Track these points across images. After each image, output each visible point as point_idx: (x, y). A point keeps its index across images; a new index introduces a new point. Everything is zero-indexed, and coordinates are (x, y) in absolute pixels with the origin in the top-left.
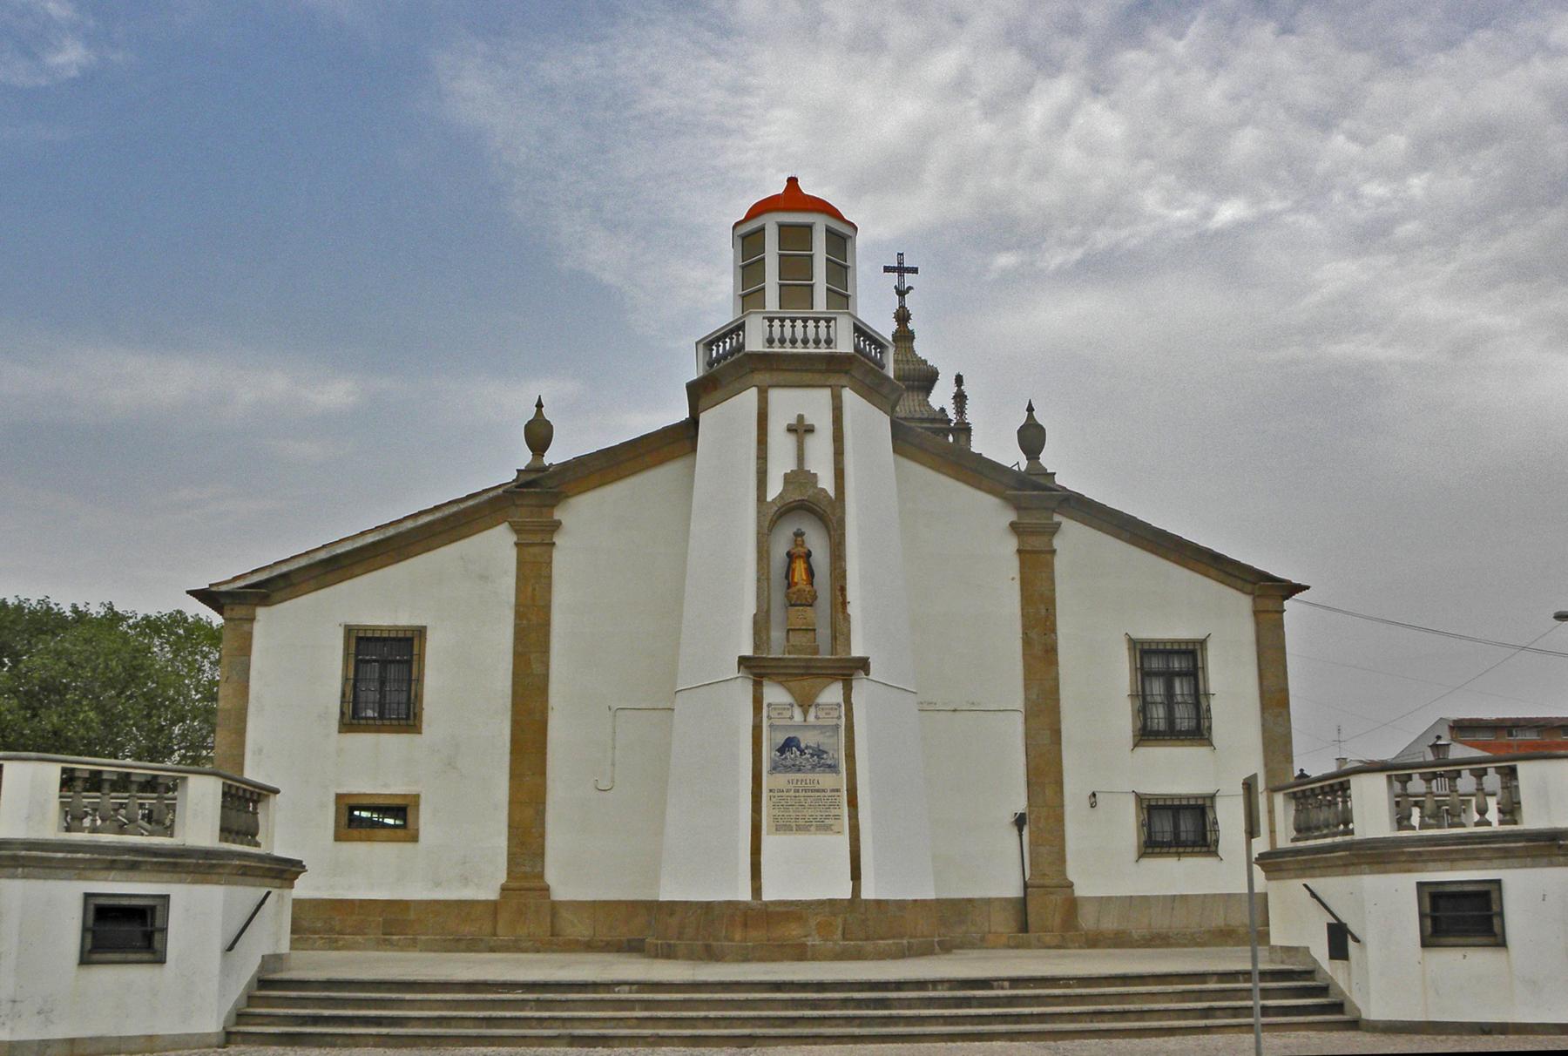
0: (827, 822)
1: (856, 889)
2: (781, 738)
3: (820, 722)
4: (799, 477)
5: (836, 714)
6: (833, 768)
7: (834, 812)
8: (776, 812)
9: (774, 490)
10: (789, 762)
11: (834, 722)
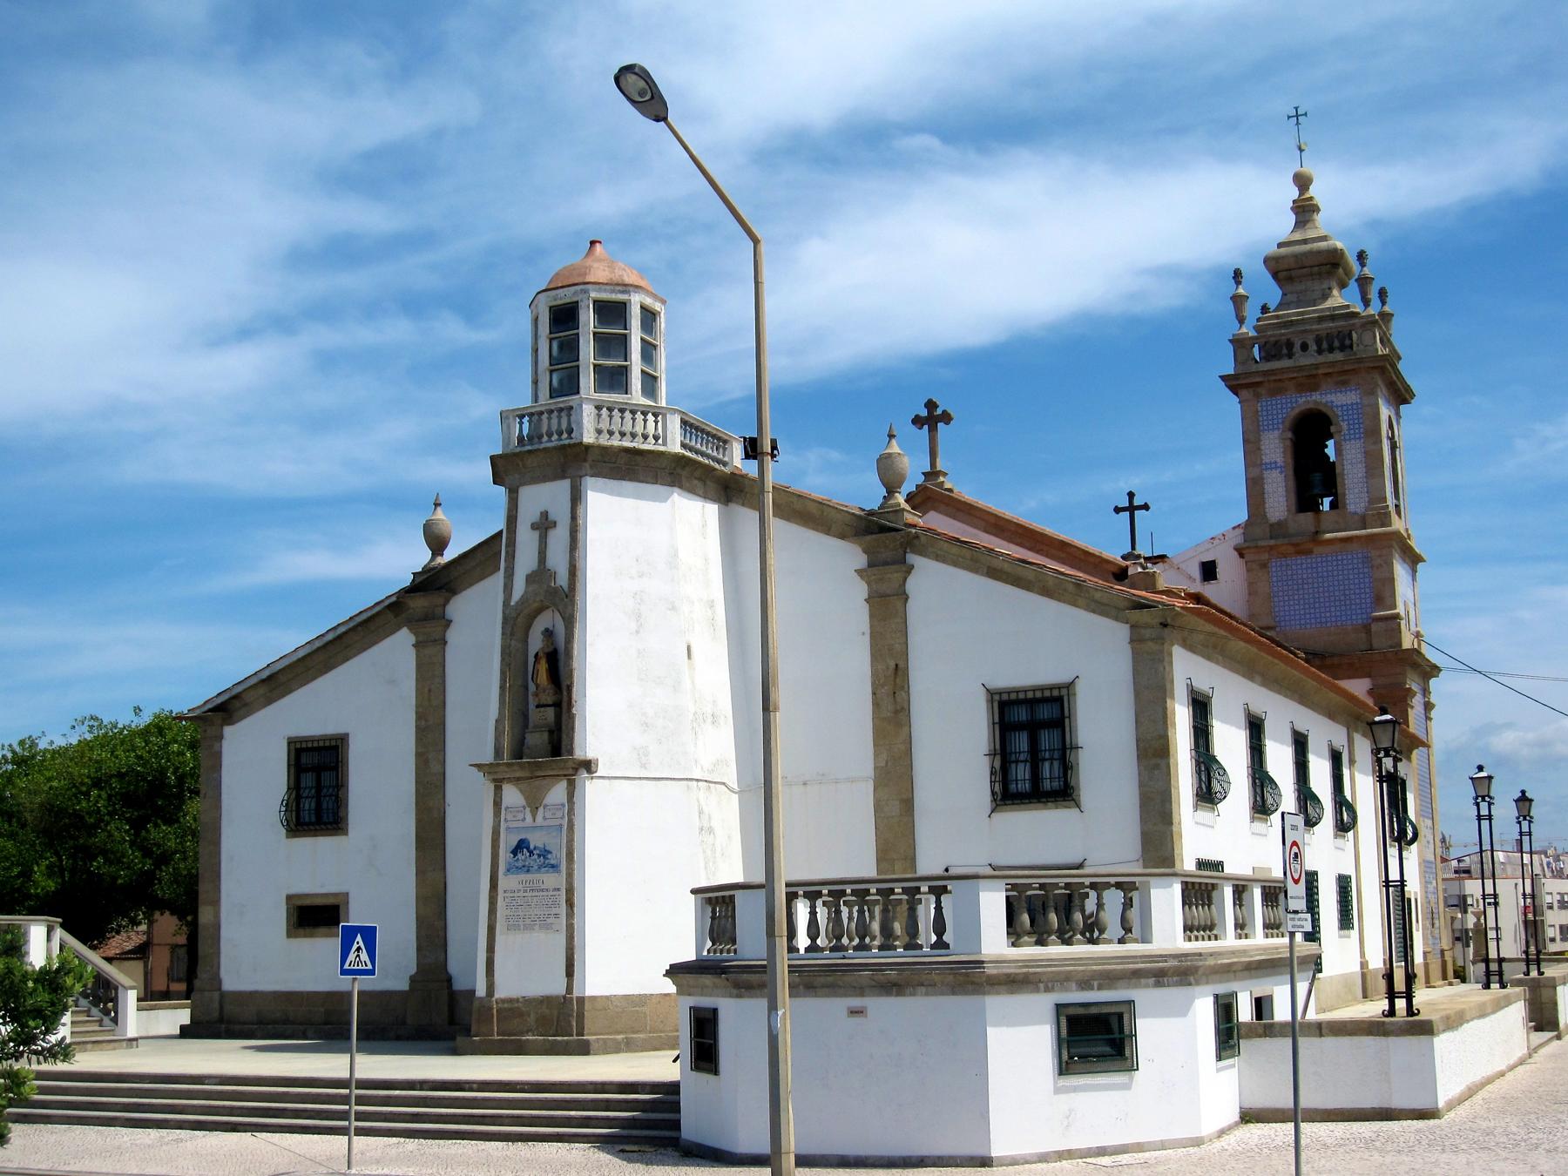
1: (569, 989)
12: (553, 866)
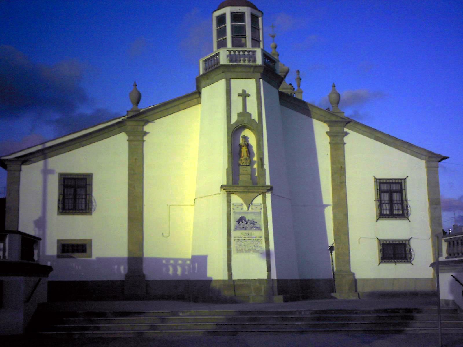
0: (257, 249)
2: (238, 217)
3: (254, 211)
4: (244, 114)
5: (259, 208)
6: (259, 228)
7: (259, 245)
8: (237, 245)
9: (234, 119)
10: (241, 226)
11: (259, 211)
12: (258, 228)
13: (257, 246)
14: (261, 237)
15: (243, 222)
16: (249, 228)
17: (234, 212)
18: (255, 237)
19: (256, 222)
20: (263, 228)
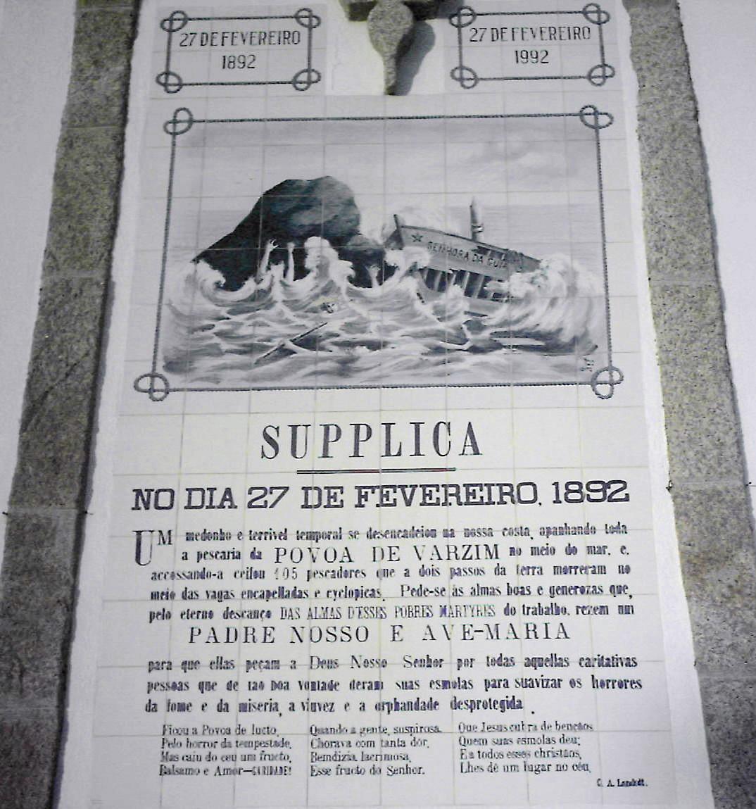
0: (542, 706)
2: (232, 198)
5: (581, 57)
7: (588, 635)
10: (276, 325)
11: (584, 94)
12: (548, 344)
13: (541, 649)
14: (611, 491)
15: (300, 255)
16: (416, 349)
17: (175, 127)
18: (511, 493)
19: (514, 260)
20: (638, 342)
